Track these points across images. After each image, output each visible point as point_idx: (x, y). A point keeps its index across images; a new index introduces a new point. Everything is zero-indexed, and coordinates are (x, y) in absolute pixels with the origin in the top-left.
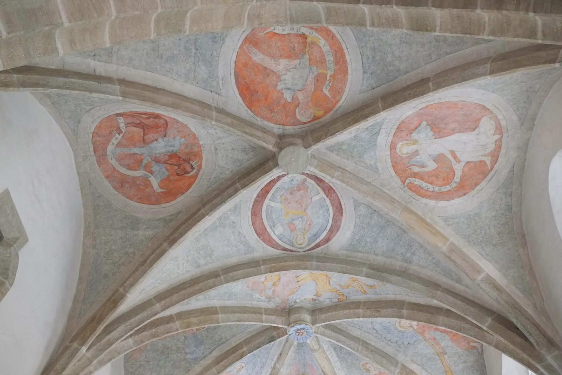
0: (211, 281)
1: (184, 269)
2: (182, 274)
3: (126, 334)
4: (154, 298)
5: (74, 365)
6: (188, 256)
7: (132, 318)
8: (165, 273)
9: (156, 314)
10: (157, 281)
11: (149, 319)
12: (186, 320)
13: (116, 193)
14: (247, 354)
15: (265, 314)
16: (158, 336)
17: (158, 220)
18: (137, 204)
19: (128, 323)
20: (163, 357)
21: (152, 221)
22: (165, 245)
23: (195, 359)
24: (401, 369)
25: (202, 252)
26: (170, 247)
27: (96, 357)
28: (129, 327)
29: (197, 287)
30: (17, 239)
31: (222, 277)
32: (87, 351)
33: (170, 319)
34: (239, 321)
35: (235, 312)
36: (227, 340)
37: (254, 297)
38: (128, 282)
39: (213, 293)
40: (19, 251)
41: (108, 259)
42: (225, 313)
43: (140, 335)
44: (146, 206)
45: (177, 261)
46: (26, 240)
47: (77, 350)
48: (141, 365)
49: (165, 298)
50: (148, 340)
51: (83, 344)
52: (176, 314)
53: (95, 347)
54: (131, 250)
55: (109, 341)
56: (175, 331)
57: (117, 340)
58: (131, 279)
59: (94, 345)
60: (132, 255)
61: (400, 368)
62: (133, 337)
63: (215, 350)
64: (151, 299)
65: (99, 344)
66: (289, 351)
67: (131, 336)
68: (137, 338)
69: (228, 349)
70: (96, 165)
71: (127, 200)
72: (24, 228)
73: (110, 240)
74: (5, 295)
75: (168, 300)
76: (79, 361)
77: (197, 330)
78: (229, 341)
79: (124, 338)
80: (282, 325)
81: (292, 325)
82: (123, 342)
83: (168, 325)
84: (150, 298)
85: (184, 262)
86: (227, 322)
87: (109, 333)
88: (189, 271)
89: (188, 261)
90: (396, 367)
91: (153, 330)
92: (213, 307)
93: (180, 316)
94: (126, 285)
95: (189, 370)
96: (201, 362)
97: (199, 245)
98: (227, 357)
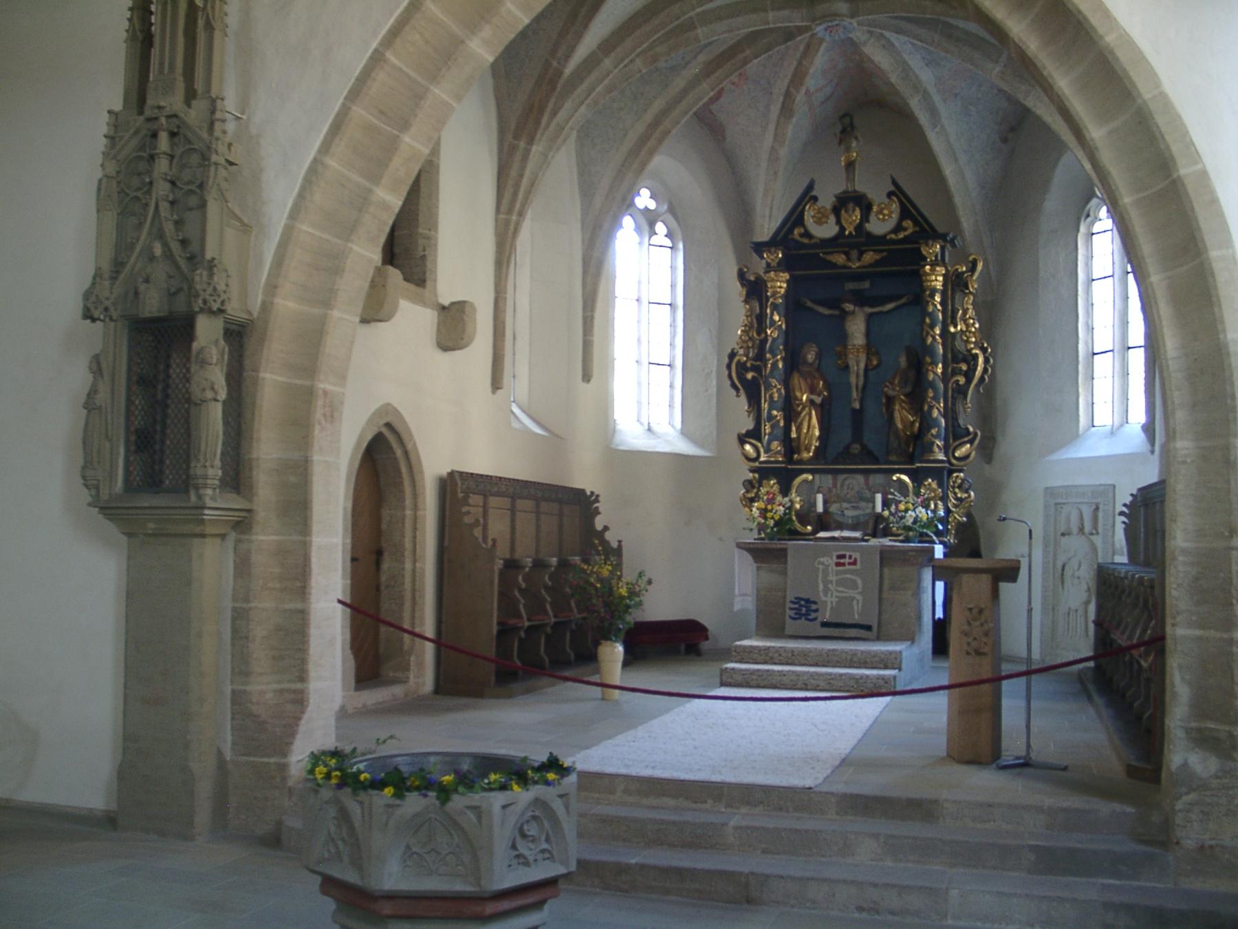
4: (598, 48)
14: (751, 60)
15: (772, 10)
24: (1005, 66)
61: (1002, 64)
66: (820, 47)
80: (802, 22)
81: (818, 22)
90: (997, 62)
95: (666, 86)
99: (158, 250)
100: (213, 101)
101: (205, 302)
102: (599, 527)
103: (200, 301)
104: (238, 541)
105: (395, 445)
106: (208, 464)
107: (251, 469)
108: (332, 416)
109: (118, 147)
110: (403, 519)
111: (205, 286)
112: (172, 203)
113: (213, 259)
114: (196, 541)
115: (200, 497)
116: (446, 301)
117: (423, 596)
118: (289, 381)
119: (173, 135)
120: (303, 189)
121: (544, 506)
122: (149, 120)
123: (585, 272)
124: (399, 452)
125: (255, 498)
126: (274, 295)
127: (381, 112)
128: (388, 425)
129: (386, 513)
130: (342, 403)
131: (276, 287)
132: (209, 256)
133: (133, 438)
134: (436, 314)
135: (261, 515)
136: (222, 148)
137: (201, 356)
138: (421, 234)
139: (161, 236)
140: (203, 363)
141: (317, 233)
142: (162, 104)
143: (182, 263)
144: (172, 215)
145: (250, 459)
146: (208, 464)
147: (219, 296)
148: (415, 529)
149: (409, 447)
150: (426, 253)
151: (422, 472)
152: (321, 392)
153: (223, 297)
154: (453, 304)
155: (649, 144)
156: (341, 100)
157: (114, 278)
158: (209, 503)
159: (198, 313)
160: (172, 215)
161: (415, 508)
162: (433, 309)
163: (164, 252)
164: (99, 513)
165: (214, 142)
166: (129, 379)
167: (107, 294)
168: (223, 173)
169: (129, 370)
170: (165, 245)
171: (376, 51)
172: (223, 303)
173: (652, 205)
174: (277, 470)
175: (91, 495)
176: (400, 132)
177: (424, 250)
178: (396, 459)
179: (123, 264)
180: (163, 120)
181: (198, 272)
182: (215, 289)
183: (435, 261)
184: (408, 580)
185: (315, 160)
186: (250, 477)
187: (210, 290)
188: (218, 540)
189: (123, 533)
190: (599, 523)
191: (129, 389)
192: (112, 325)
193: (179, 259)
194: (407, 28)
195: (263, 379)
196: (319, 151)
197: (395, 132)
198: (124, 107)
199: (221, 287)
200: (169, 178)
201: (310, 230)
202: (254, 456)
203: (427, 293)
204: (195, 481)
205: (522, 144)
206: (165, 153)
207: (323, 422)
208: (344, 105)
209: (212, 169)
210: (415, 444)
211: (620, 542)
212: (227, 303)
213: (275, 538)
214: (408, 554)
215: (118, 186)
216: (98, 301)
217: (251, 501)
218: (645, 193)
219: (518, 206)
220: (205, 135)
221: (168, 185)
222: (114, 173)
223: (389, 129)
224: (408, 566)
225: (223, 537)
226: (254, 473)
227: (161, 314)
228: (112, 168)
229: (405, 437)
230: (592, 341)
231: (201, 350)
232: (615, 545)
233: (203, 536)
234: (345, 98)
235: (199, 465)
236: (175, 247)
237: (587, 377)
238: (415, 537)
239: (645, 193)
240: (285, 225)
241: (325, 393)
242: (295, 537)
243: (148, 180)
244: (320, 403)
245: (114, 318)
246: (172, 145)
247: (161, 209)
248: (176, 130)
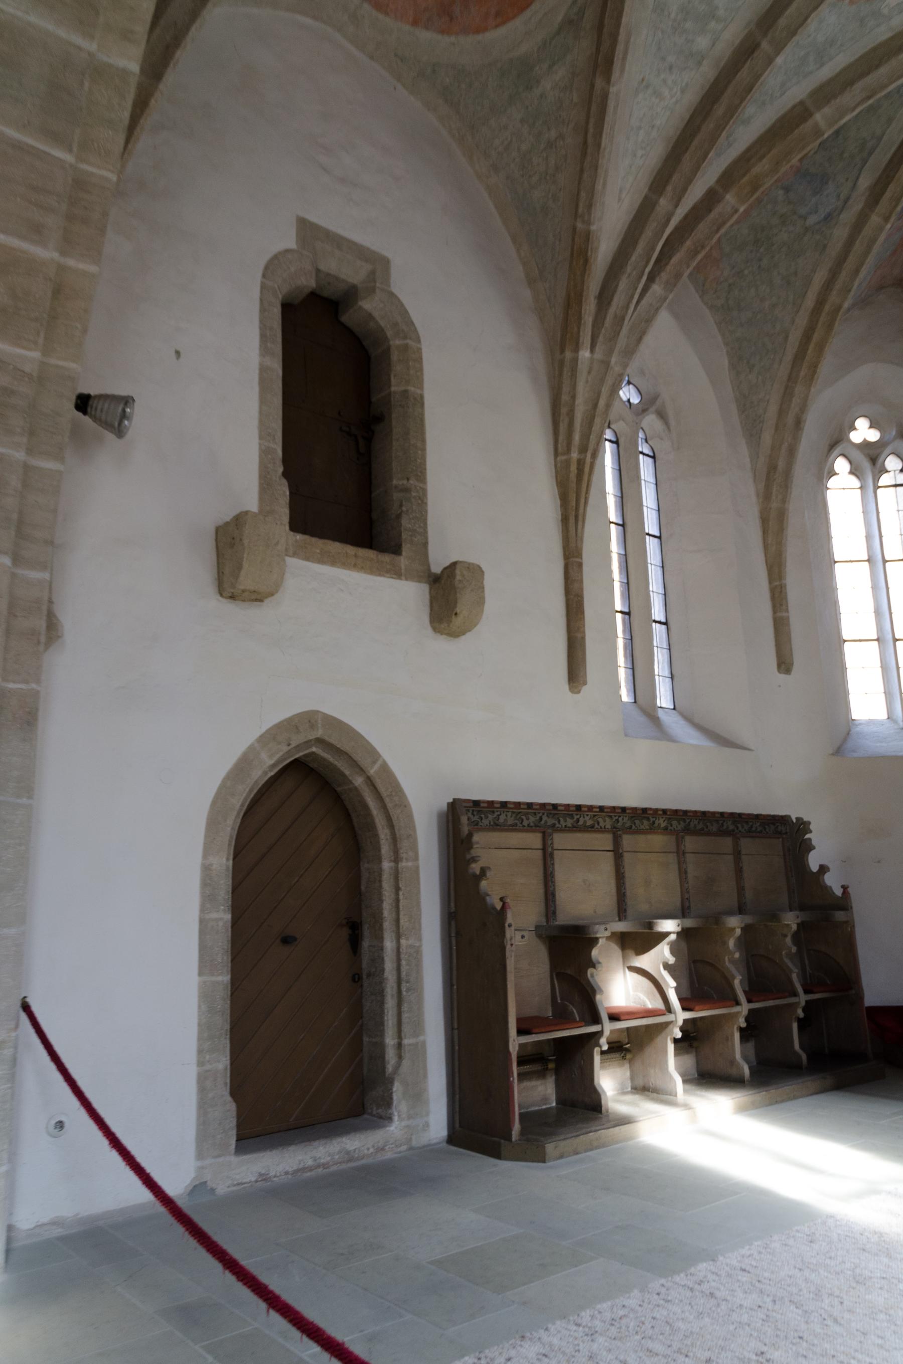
0: (744, 74)
1: (675, 90)
2: (677, 102)
3: (636, 289)
4: (650, 189)
5: (587, 382)
6: (663, 59)
7: (632, 255)
8: (640, 128)
9: (668, 221)
10: (635, 155)
11: (660, 239)
12: (746, 179)
13: (453, 39)
16: (703, 247)
17: (558, 33)
18: (502, 31)
19: (629, 269)
20: (762, 250)
21: (550, 44)
22: (599, 83)
23: (828, 218)
25: (688, 25)
26: (608, 81)
27: (610, 352)
28: (634, 273)
29: (720, 110)
30: (373, 272)
31: (765, 45)
32: (592, 350)
33: (711, 198)
34: (869, 98)
35: (852, 83)
36: (880, 139)
37: (885, 11)
38: (581, 205)
39: (772, 80)
40: (389, 286)
41: (530, 176)
42: (828, 102)
43: (668, 268)
44: (517, 24)
45: (647, 87)
46: (385, 263)
47: (575, 360)
48: (730, 285)
49: (670, 176)
50: (688, 267)
51: (576, 349)
52: (718, 181)
53: (601, 338)
54: (553, 134)
55: (616, 316)
56: (732, 215)
57: (627, 308)
58: (583, 194)
59: (598, 337)
60: (561, 143)
62: (657, 280)
63: (862, 176)
64: (646, 197)
65: (603, 331)
67: (651, 279)
68: (664, 276)
69: (889, 156)
70: (381, 16)
71: (480, 37)
72: (368, 249)
73: (509, 139)
74: (421, 359)
75: (675, 178)
76: (589, 372)
77: (801, 160)
78: (885, 138)
79: (636, 297)
82: (644, 302)
83: (713, 215)
84: (643, 195)
85: (663, 76)
86: (841, 118)
87: (609, 304)
88: (687, 85)
89: (671, 68)
91: (688, 243)
92: (794, 107)
93: (728, 179)
94: (580, 210)
95: (825, 247)
96: (841, 216)
97: (673, 16)
98: (894, 177)
102: (814, 868)
110: (380, 875)
116: (436, 569)
117: (417, 988)
121: (690, 843)
123: (765, 532)
124: (359, 781)
129: (365, 866)
138: (396, 487)
155: (816, 336)
162: (419, 582)
173: (873, 436)
177: (401, 506)
184: (389, 966)
190: (814, 862)
205: (568, 355)
210: (385, 768)
211: (845, 888)
214: (388, 925)
218: (862, 424)
219: (577, 438)
224: (389, 944)
230: (788, 618)
232: (838, 892)
237: (784, 665)
238: (397, 901)
239: (862, 424)
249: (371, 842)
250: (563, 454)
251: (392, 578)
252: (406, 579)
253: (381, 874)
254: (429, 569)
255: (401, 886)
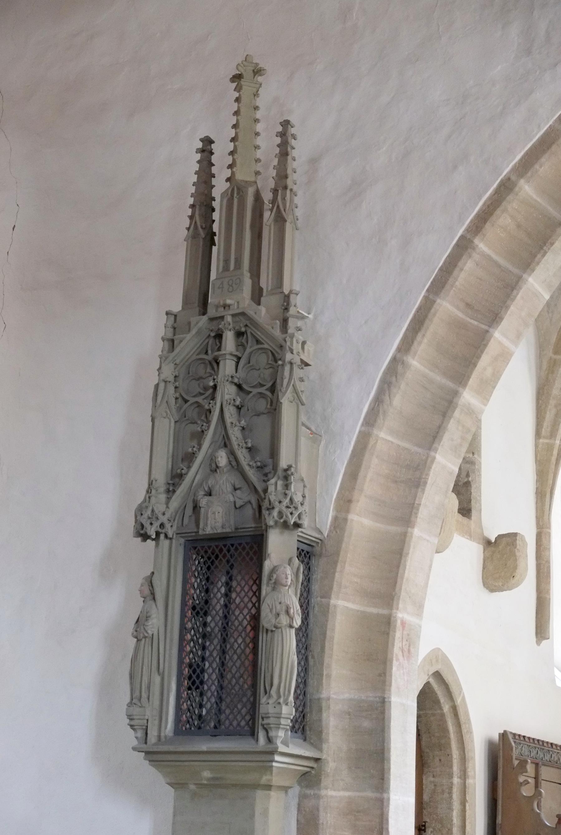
99: (222, 459)
100: (287, 298)
101: (280, 514)
103: (275, 513)
104: (302, 797)
105: (442, 700)
106: (281, 700)
107: (320, 710)
108: (409, 651)
109: (177, 350)
110: (451, 788)
111: (281, 497)
112: (239, 408)
113: (290, 467)
114: (260, 794)
115: (269, 740)
118: (362, 608)
119: (239, 334)
120: (381, 392)
122: (212, 319)
124: (446, 708)
125: (325, 746)
126: (348, 511)
127: (468, 305)
128: (437, 675)
130: (419, 637)
131: (350, 501)
132: (283, 463)
133: (186, 671)
134: (481, 547)
135: (331, 766)
136: (296, 347)
137: (275, 576)
139: (226, 443)
140: (276, 585)
141: (396, 441)
142: (229, 302)
143: (252, 474)
144: (239, 421)
145: (319, 699)
146: (281, 700)
147: (296, 508)
148: (463, 803)
149: (459, 701)
150: (470, 479)
151: (470, 732)
152: (399, 622)
153: (300, 509)
154: (500, 537)
156: (423, 293)
157: (170, 491)
158: (282, 748)
159: (271, 527)
160: (239, 421)
161: (464, 775)
162: (479, 543)
163: (230, 463)
164: (145, 759)
165: (288, 339)
166: (184, 603)
167: (162, 508)
168: (298, 374)
169: (185, 593)
170: (232, 454)
171: (462, 237)
172: (299, 516)
174: (349, 714)
175: (136, 738)
176: (490, 326)
177: (468, 475)
178: (443, 715)
179: (181, 476)
180: (229, 319)
181: (273, 481)
182: (291, 500)
183: (479, 488)
185: (394, 360)
186: (320, 720)
187: (286, 502)
188: (282, 794)
189: (168, 784)
191: (183, 615)
192: (167, 542)
193: (247, 468)
194: (498, 212)
195: (335, 606)
196: (399, 350)
197: (483, 327)
198: (183, 308)
199: (298, 498)
200: (236, 380)
201: (389, 438)
202: (324, 695)
203: (472, 523)
204: (266, 721)
206: (231, 354)
207: (401, 658)
208: (426, 298)
209: (287, 368)
210: (464, 699)
212: (304, 517)
213: (347, 794)
215: (175, 392)
216: (154, 516)
217: (320, 750)
220: (277, 333)
221: (234, 389)
222: (171, 379)
223: (476, 323)
225: (285, 789)
226: (324, 715)
227: (228, 530)
228: (168, 372)
229: (453, 688)
231: (274, 570)
233: (268, 787)
234: (428, 290)
235: (271, 701)
236: (243, 456)
240: (360, 432)
241: (403, 624)
242: (370, 794)
243: (211, 384)
244: (398, 634)
245: (170, 535)
246: (241, 346)
247: (227, 415)
248: (243, 330)
249: (440, 760)
250: (545, 438)
251: (467, 538)
252: (474, 541)
253: (452, 787)
254: (483, 534)
255: (467, 798)
